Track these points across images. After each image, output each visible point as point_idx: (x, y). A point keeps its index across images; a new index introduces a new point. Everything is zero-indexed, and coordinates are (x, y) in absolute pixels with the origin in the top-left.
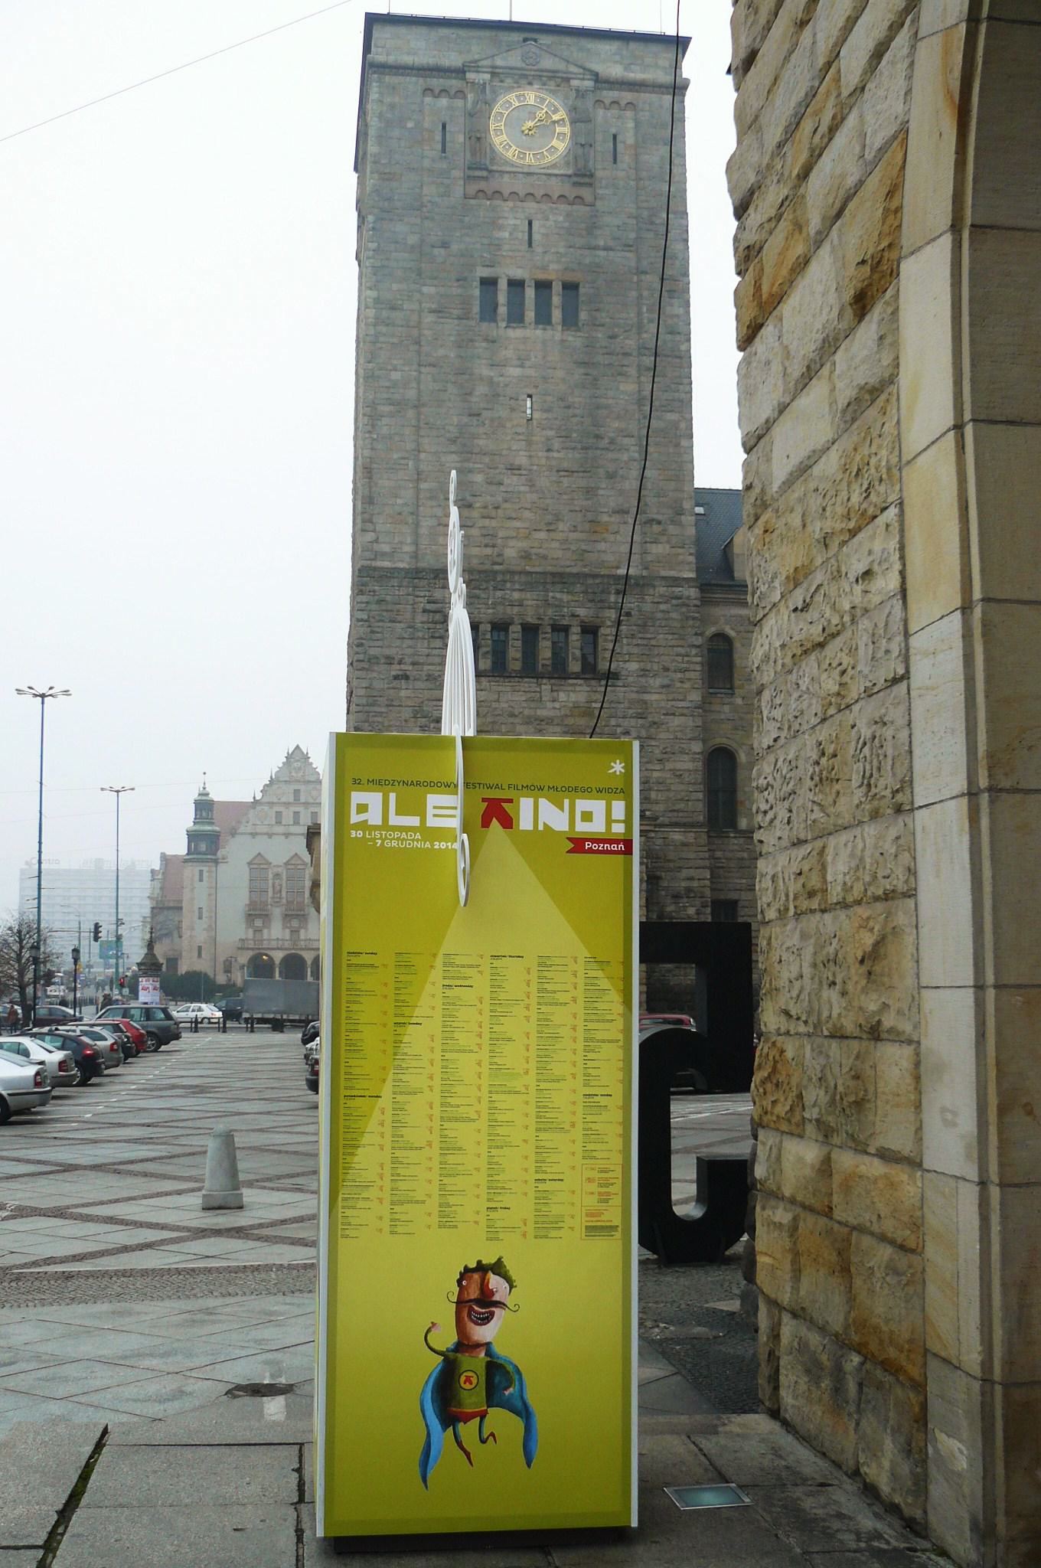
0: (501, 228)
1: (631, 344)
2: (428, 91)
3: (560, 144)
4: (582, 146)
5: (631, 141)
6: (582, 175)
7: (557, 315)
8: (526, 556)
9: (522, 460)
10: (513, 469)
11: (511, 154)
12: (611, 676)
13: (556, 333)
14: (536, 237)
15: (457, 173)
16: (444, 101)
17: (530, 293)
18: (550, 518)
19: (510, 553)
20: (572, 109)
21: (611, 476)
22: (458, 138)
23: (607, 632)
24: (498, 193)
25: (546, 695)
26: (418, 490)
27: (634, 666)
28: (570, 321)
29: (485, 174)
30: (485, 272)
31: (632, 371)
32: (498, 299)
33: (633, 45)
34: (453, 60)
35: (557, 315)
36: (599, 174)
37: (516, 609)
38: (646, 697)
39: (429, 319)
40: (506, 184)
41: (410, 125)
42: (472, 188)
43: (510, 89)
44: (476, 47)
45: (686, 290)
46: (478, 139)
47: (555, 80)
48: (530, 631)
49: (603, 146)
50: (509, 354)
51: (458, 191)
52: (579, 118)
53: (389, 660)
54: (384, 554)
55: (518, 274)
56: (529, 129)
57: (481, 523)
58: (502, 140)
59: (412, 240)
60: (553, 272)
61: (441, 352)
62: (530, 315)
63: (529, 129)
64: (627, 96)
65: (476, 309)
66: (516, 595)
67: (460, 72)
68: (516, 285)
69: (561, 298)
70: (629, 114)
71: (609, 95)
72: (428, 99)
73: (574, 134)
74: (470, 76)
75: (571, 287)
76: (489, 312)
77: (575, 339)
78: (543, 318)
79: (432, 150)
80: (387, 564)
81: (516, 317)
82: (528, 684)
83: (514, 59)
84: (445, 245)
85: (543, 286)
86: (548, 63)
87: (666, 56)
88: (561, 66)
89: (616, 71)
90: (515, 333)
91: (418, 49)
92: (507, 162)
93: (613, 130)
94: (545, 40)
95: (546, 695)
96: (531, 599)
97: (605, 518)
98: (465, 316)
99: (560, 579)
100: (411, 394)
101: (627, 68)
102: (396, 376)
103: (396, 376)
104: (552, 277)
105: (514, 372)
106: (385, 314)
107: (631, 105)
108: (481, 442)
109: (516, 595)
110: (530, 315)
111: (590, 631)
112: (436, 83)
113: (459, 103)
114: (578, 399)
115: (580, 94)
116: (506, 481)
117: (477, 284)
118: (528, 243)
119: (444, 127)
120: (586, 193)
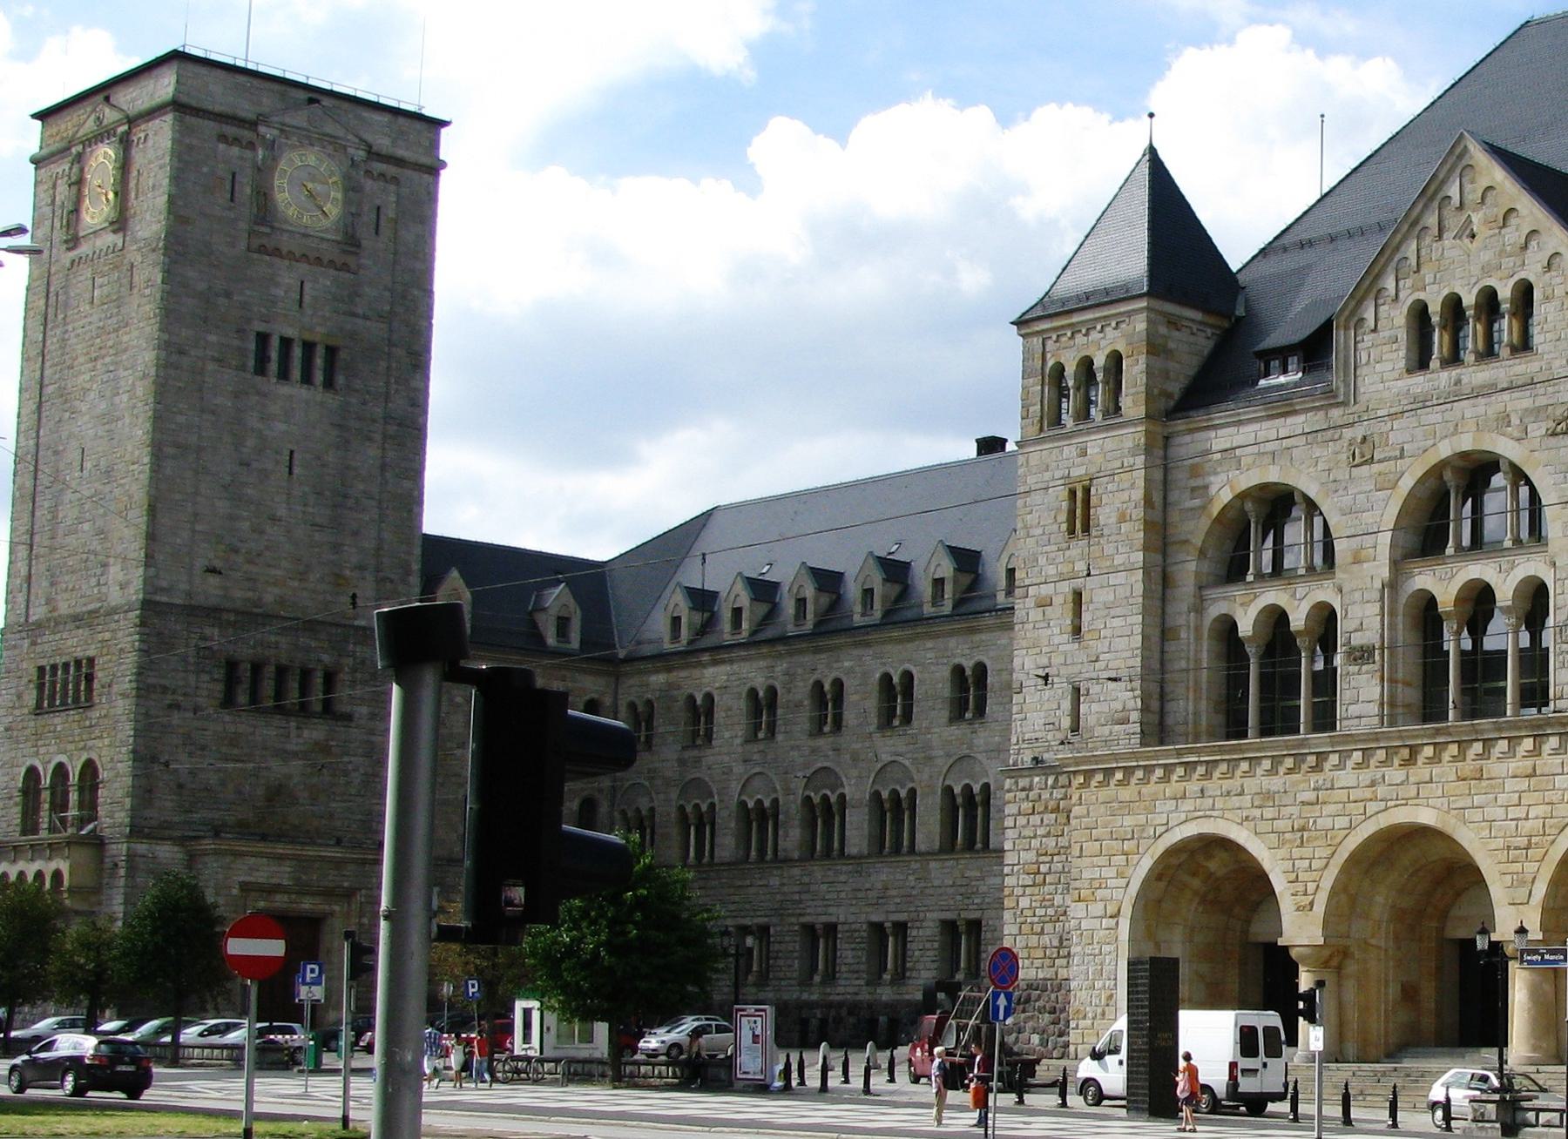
0: (277, 285)
1: (378, 411)
2: (223, 138)
3: (334, 211)
4: (352, 216)
5: (391, 214)
6: (351, 242)
7: (319, 377)
8: (281, 601)
9: (282, 512)
10: (274, 519)
11: (291, 212)
12: (348, 717)
13: (316, 394)
14: (307, 299)
15: (243, 226)
16: (235, 150)
17: (297, 352)
18: (301, 568)
19: (268, 598)
20: (347, 177)
21: (355, 534)
23: (344, 676)
24: (276, 252)
25: (294, 733)
26: (194, 531)
27: (364, 710)
28: (329, 384)
29: (267, 230)
30: (262, 327)
31: (378, 437)
32: (270, 356)
33: (401, 120)
34: (246, 110)
35: (319, 377)
36: (364, 243)
37: (273, 651)
38: (373, 738)
39: (211, 366)
40: (286, 243)
41: (205, 170)
42: (256, 242)
43: (293, 147)
44: (268, 101)
45: (428, 368)
46: (263, 196)
47: (333, 144)
48: (281, 671)
49: (369, 217)
50: (275, 408)
51: (243, 245)
52: (352, 188)
53: (165, 689)
54: (162, 589)
55: (290, 332)
57: (246, 567)
58: (285, 197)
59: (202, 286)
60: (319, 334)
61: (218, 401)
62: (296, 373)
63: (307, 191)
64: (392, 170)
65: (251, 363)
66: (273, 639)
67: (253, 125)
68: (286, 343)
69: (321, 362)
70: (393, 188)
71: (379, 167)
72: (222, 146)
73: (347, 202)
74: (262, 129)
75: (331, 351)
76: (261, 369)
77: (333, 401)
78: (307, 379)
79: (222, 197)
80: (164, 599)
81: (284, 375)
82: (277, 720)
84: (228, 295)
85: (309, 347)
86: (330, 128)
88: (341, 133)
89: (383, 143)
90: (285, 389)
91: (218, 95)
92: (286, 221)
93: (378, 202)
94: (326, 102)
95: (294, 733)
96: (284, 642)
97: (347, 573)
98: (243, 368)
99: (311, 626)
100: (193, 439)
101: (394, 142)
102: (181, 419)
103: (181, 419)
104: (317, 338)
105: (282, 427)
106: (174, 358)
107: (395, 180)
108: (249, 491)
109: (273, 639)
110: (296, 373)
111: (330, 679)
112: (231, 130)
113: (248, 154)
114: (331, 457)
115: (353, 164)
116: (268, 529)
117: (252, 337)
118: (298, 304)
119: (234, 175)
120: (351, 260)
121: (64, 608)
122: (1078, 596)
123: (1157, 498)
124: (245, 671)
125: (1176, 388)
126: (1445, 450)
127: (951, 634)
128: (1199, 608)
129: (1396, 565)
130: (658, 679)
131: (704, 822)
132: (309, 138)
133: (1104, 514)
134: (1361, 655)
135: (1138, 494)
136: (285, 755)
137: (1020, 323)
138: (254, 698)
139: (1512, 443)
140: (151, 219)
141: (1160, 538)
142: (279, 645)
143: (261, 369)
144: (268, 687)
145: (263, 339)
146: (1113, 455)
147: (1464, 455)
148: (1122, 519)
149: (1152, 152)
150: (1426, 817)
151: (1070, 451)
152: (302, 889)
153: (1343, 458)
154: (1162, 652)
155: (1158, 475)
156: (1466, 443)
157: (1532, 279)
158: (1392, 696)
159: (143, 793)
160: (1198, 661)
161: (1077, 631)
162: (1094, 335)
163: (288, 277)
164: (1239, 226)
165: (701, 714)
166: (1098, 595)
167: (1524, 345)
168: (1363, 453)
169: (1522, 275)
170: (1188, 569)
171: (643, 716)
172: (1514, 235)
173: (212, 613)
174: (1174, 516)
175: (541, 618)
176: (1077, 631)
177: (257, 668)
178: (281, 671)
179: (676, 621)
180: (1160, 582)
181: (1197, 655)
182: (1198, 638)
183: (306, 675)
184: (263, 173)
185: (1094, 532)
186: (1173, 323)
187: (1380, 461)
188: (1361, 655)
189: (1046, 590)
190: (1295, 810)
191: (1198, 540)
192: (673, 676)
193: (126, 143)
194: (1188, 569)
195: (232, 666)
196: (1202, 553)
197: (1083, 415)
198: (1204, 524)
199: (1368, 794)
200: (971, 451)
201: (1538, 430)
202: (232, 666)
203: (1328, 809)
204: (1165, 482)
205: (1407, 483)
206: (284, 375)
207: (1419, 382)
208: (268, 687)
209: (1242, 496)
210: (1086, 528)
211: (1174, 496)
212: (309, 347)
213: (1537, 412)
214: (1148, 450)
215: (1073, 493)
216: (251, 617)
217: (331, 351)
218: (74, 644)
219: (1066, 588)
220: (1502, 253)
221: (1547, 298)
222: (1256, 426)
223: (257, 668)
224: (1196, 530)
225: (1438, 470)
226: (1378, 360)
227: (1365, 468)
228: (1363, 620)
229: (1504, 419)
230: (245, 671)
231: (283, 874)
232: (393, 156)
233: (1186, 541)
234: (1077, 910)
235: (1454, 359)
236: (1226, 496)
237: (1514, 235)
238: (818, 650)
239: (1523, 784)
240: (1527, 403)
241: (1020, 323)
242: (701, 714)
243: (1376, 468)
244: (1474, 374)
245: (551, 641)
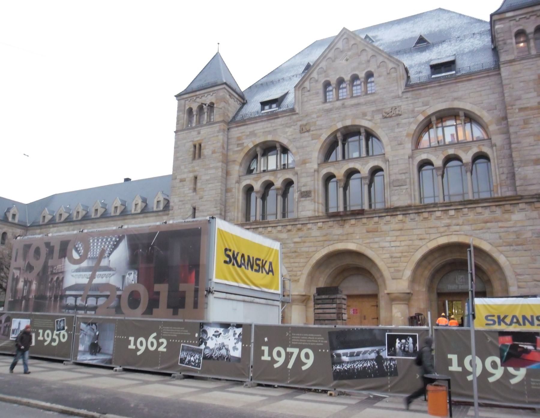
122: (196, 178)
123: (225, 146)
126: (340, 125)
127: (119, 220)
128: (238, 182)
133: (206, 151)
134: (306, 194)
135: (219, 145)
137: (176, 96)
139: (367, 122)
147: (346, 127)
148: (214, 152)
149: (218, 52)
150: (351, 246)
151: (194, 133)
154: (226, 196)
155: (226, 140)
156: (348, 123)
157: (373, 70)
158: (318, 208)
160: (238, 200)
161: (195, 190)
162: (204, 98)
166: (203, 178)
168: (304, 130)
169: (369, 69)
170: (236, 169)
172: (364, 58)
174: (230, 153)
175: (8, 214)
176: (195, 190)
179: (44, 217)
181: (239, 196)
182: (239, 192)
185: (202, 157)
186: (231, 95)
187: (312, 131)
188: (306, 194)
189: (184, 176)
190: (292, 245)
191: (239, 160)
196: (241, 165)
197: (199, 122)
198: (242, 155)
199: (324, 238)
200: (123, 181)
201: (378, 117)
203: (307, 244)
204: (228, 142)
207: (327, 106)
209: (256, 146)
210: (200, 156)
211: (230, 147)
213: (378, 111)
215: (195, 146)
219: (191, 175)
220: (360, 63)
221: (380, 76)
222: (263, 123)
225: (335, 133)
227: (306, 134)
229: (364, 114)
233: (234, 161)
236: (251, 145)
237: (364, 58)
238: (82, 224)
239: (398, 233)
240: (374, 109)
241: (176, 96)
243: (311, 132)
245: (10, 219)
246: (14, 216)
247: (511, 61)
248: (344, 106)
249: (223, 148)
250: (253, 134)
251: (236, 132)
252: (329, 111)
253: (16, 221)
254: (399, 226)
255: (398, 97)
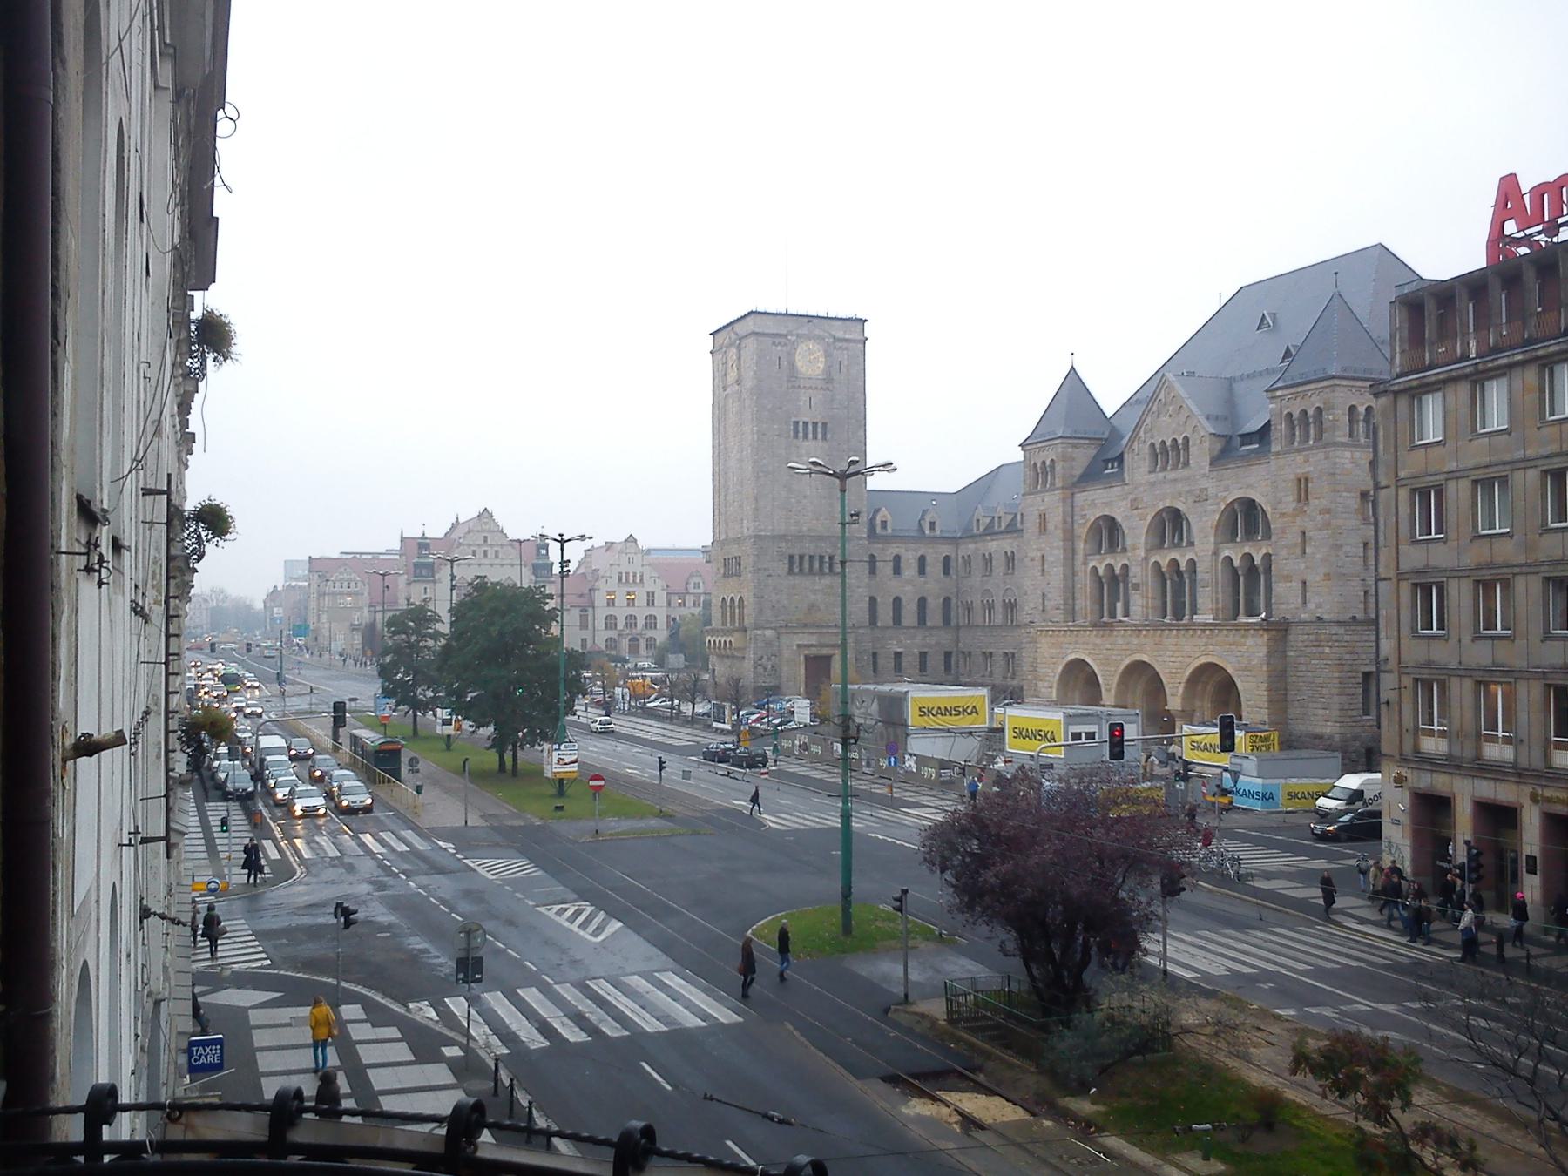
4: (829, 367)
6: (828, 379)
13: (820, 442)
22: (784, 363)
28: (824, 438)
32: (800, 430)
46: (792, 365)
47: (820, 338)
48: (811, 557)
52: (828, 355)
56: (810, 360)
58: (800, 363)
60: (818, 419)
63: (810, 360)
64: (845, 345)
68: (806, 424)
69: (821, 430)
75: (824, 425)
76: (796, 436)
83: (804, 331)
85: (815, 424)
86: (817, 332)
87: (859, 325)
89: (840, 334)
91: (770, 326)
99: (821, 538)
112: (777, 340)
118: (809, 408)
121: (731, 535)
124: (797, 558)
125: (1078, 472)
128: (1085, 564)
129: (1147, 551)
130: (972, 546)
131: (991, 607)
132: (809, 337)
133: (1050, 526)
134: (1136, 587)
136: (815, 592)
138: (801, 570)
140: (748, 376)
141: (1070, 537)
142: (809, 548)
143: (796, 436)
144: (806, 566)
145: (796, 423)
146: (1052, 502)
150: (1145, 658)
152: (821, 646)
153: (1132, 501)
159: (761, 612)
163: (804, 397)
164: (1111, 396)
165: (988, 560)
167: (1186, 464)
171: (968, 561)
173: (782, 537)
177: (801, 557)
178: (811, 557)
180: (1071, 553)
181: (1085, 583)
183: (821, 557)
184: (791, 355)
186: (1075, 446)
188: (1136, 587)
192: (980, 545)
193: (739, 349)
194: (1080, 546)
195: (791, 557)
201: (1191, 500)
202: (791, 557)
205: (1149, 518)
206: (805, 437)
208: (806, 566)
212: (815, 424)
214: (1064, 500)
216: (800, 537)
217: (824, 425)
218: (734, 551)
223: (801, 557)
224: (1082, 531)
226: (1138, 467)
228: (1136, 575)
230: (797, 558)
231: (813, 640)
232: (844, 338)
234: (1040, 684)
235: (1164, 469)
242: (988, 560)
244: (1171, 475)
246: (932, 524)
247: (1278, 453)
248: (1164, 481)
249: (1065, 522)
250: (1093, 504)
251: (1081, 498)
252: (1152, 484)
253: (938, 533)
254: (1174, 641)
255: (1204, 476)
